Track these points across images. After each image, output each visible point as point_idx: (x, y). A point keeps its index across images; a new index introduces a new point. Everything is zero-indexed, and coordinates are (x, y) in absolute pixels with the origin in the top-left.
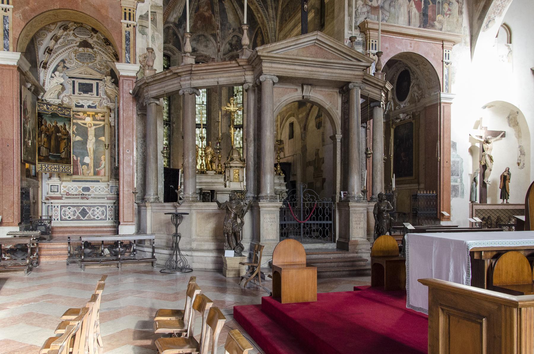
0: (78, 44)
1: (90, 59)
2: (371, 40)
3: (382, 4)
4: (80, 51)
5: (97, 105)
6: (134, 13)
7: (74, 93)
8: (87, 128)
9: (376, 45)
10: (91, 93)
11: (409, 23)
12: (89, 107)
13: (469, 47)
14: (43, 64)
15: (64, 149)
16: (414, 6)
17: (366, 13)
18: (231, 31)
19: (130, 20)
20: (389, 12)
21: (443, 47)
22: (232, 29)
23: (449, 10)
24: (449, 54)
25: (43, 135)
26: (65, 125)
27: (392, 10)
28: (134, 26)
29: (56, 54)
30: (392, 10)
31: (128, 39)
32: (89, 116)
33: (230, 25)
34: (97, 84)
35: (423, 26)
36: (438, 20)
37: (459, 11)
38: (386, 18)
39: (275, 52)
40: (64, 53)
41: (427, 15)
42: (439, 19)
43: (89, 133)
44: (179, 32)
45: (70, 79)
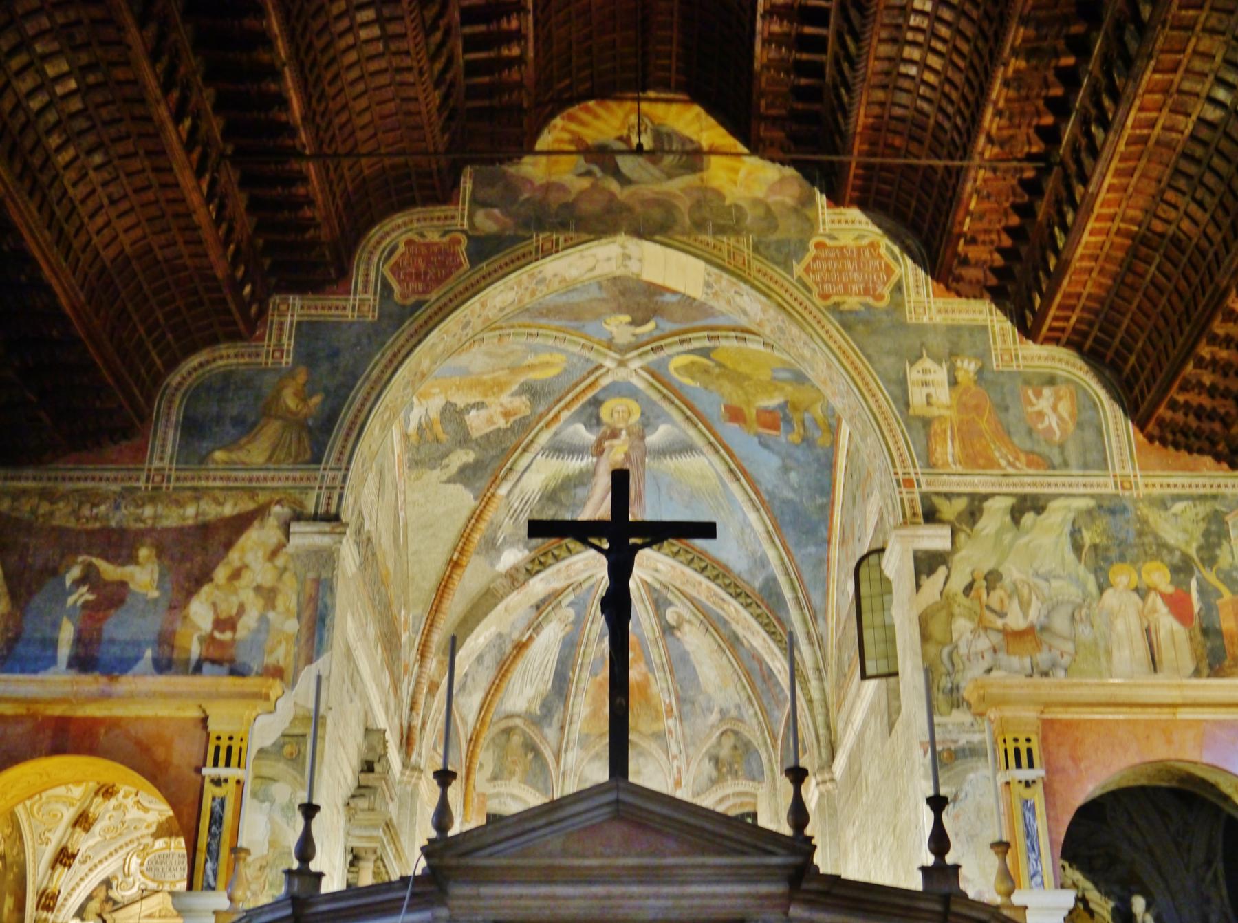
0: (153, 829)
3: (1042, 618)
6: (244, 745)
9: (1029, 751)
11: (1154, 664)
17: (988, 656)
18: (714, 717)
19: (228, 764)
22: (716, 709)
27: (1084, 632)
28: (238, 782)
29: (89, 864)
30: (1084, 632)
31: (217, 820)
33: (709, 699)
35: (1211, 667)
39: (483, 853)
40: (111, 860)
41: (1219, 633)
44: (545, 738)
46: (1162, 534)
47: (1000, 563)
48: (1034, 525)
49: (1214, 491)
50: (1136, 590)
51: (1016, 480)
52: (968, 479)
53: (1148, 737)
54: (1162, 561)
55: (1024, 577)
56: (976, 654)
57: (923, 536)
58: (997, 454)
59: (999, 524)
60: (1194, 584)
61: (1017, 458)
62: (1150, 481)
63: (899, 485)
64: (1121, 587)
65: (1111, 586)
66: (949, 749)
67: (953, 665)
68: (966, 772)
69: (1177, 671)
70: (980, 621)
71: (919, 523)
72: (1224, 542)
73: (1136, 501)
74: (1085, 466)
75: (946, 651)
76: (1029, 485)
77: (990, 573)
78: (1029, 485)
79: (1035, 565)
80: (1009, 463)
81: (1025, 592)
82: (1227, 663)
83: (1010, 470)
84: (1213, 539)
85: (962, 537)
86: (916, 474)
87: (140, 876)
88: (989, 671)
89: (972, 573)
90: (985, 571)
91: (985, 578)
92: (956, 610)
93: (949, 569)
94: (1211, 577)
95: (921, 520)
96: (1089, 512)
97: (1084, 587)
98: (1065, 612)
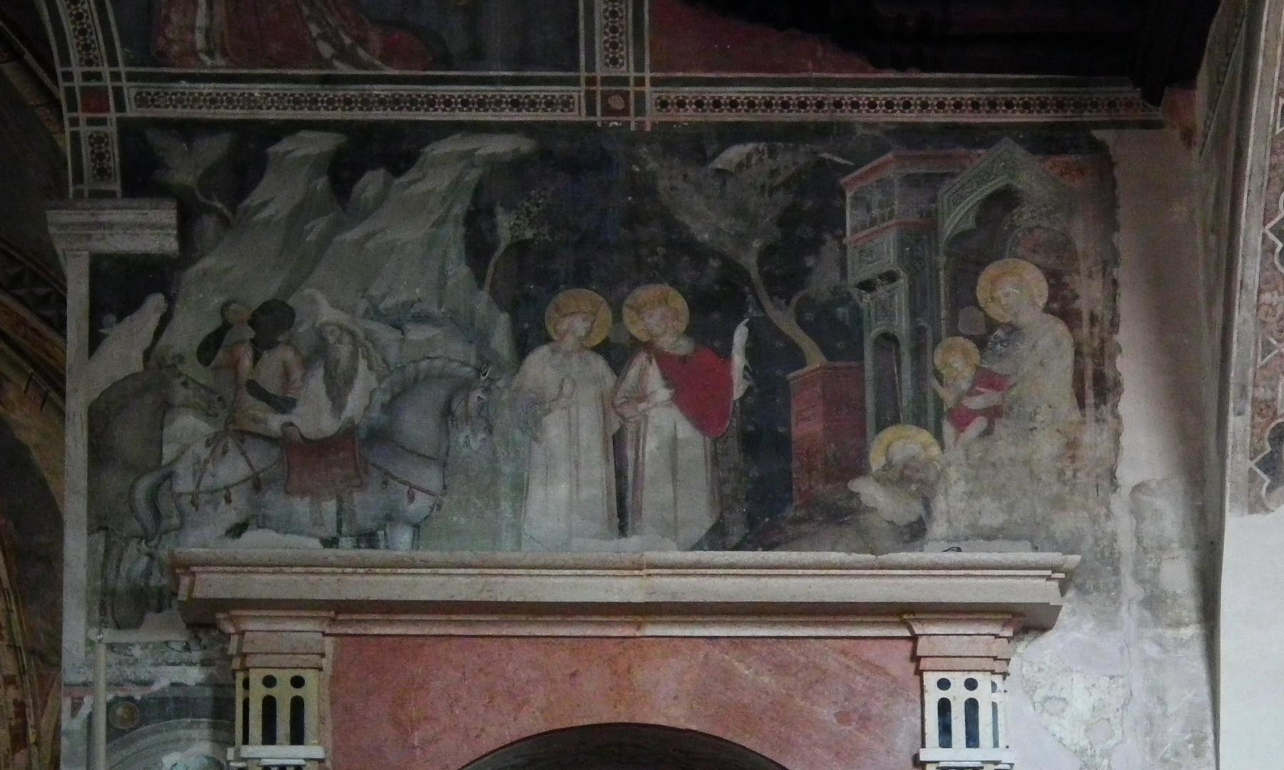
2: (256, 677)
3: (375, 414)
13: (1192, 631)
16: (663, 394)
17: (238, 498)
20: (443, 462)
21: (915, 658)
23: (986, 379)
24: (972, 706)
30: (469, 442)
35: (751, 521)
36: (889, 465)
37: (1078, 378)
38: (422, 503)
41: (782, 445)
42: (898, 455)
46: (686, 219)
47: (291, 288)
48: (381, 200)
49: (822, 117)
50: (604, 349)
51: (352, 91)
52: (242, 87)
53: (574, 675)
54: (674, 284)
55: (342, 318)
56: (213, 492)
57: (111, 226)
58: (314, 30)
59: (298, 198)
60: (740, 336)
61: (362, 41)
62: (674, 93)
63: (72, 108)
64: (570, 342)
65: (548, 340)
66: (130, 699)
67: (157, 515)
68: (165, 747)
69: (671, 530)
70: (232, 420)
71: (111, 195)
72: (830, 243)
73: (634, 139)
74: (522, 59)
75: (144, 484)
76: (382, 102)
77: (266, 308)
78: (382, 102)
79: (375, 292)
80: (344, 54)
81: (344, 351)
82: (790, 512)
83: (343, 69)
84: (807, 232)
85: (209, 224)
86: (116, 76)
88: (237, 530)
89: (225, 306)
90: (256, 303)
91: (253, 322)
92: (180, 394)
93: (171, 300)
94: (785, 321)
95: (116, 187)
96: (516, 166)
97: (481, 339)
98: (432, 396)
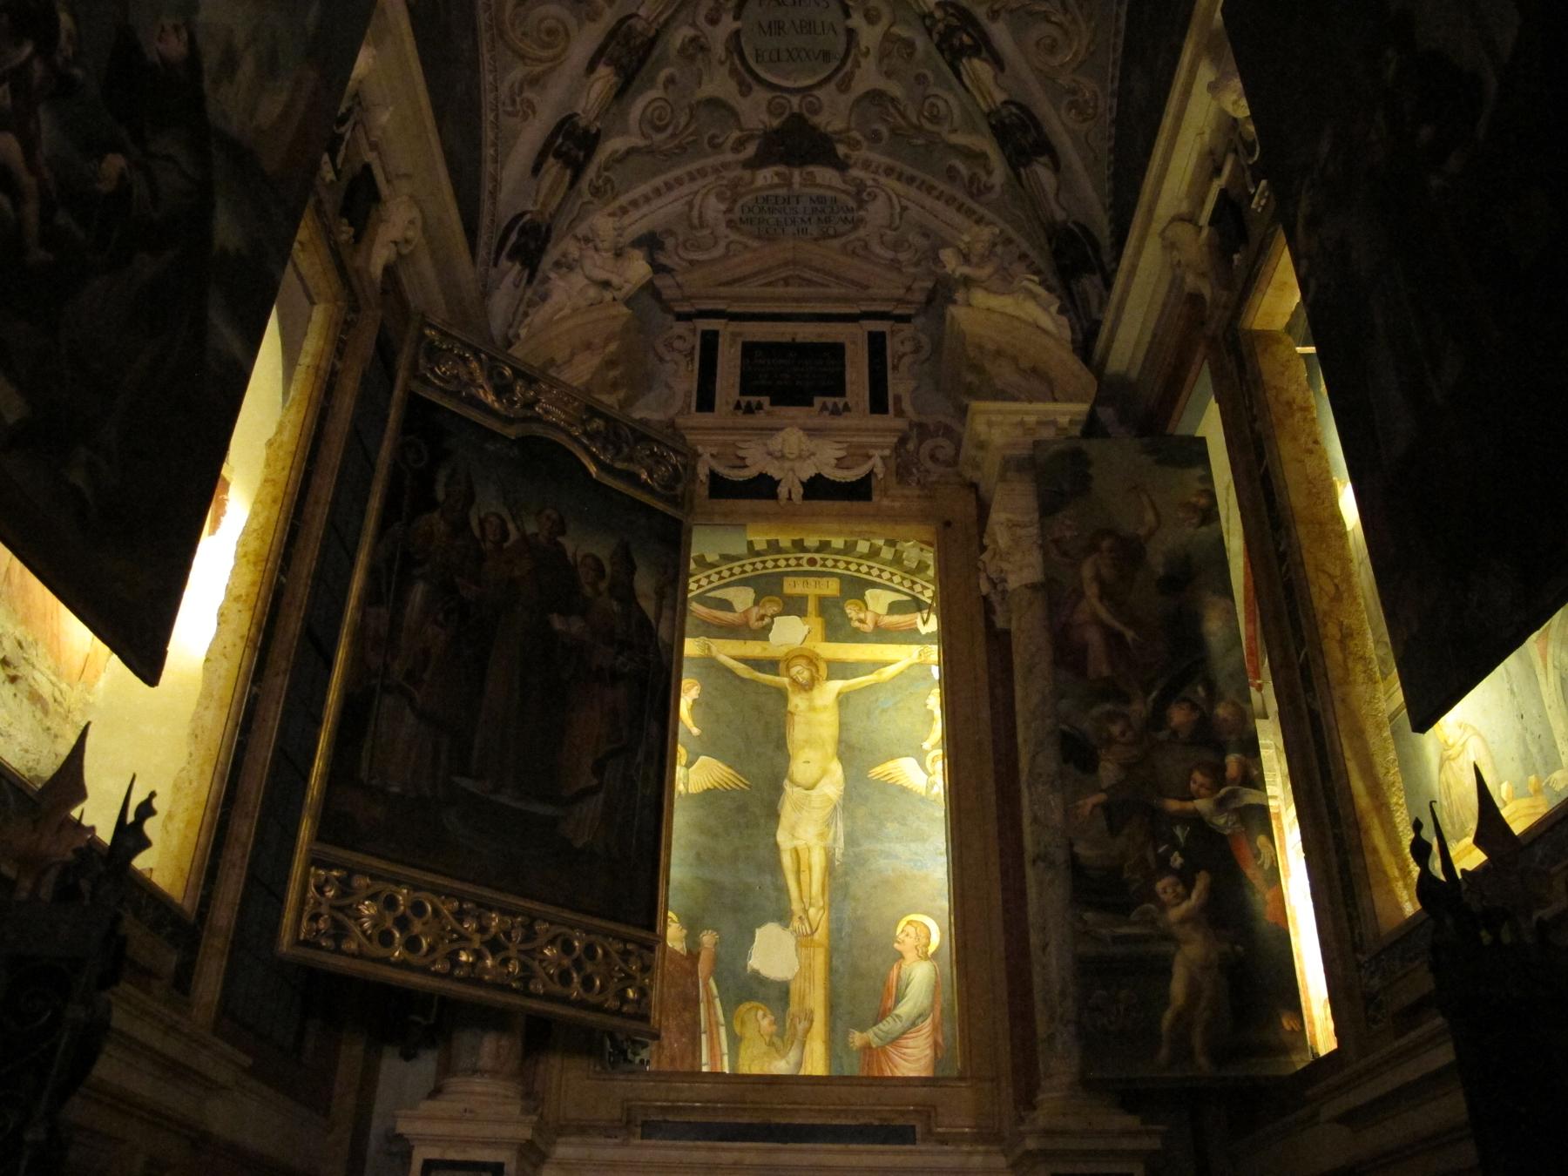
0: (751, 150)
1: (828, 220)
4: (760, 182)
5: (880, 471)
7: (706, 401)
8: (781, 695)
10: (830, 401)
12: (817, 488)
14: (523, 232)
15: (599, 768)
25: (418, 592)
26: (627, 564)
32: (795, 606)
34: (877, 343)
43: (798, 733)
45: (681, 328)
87: (728, 232)
